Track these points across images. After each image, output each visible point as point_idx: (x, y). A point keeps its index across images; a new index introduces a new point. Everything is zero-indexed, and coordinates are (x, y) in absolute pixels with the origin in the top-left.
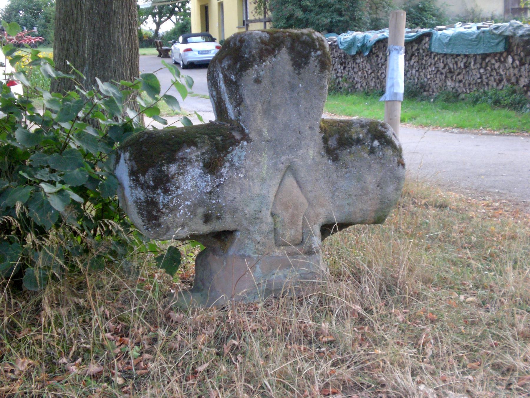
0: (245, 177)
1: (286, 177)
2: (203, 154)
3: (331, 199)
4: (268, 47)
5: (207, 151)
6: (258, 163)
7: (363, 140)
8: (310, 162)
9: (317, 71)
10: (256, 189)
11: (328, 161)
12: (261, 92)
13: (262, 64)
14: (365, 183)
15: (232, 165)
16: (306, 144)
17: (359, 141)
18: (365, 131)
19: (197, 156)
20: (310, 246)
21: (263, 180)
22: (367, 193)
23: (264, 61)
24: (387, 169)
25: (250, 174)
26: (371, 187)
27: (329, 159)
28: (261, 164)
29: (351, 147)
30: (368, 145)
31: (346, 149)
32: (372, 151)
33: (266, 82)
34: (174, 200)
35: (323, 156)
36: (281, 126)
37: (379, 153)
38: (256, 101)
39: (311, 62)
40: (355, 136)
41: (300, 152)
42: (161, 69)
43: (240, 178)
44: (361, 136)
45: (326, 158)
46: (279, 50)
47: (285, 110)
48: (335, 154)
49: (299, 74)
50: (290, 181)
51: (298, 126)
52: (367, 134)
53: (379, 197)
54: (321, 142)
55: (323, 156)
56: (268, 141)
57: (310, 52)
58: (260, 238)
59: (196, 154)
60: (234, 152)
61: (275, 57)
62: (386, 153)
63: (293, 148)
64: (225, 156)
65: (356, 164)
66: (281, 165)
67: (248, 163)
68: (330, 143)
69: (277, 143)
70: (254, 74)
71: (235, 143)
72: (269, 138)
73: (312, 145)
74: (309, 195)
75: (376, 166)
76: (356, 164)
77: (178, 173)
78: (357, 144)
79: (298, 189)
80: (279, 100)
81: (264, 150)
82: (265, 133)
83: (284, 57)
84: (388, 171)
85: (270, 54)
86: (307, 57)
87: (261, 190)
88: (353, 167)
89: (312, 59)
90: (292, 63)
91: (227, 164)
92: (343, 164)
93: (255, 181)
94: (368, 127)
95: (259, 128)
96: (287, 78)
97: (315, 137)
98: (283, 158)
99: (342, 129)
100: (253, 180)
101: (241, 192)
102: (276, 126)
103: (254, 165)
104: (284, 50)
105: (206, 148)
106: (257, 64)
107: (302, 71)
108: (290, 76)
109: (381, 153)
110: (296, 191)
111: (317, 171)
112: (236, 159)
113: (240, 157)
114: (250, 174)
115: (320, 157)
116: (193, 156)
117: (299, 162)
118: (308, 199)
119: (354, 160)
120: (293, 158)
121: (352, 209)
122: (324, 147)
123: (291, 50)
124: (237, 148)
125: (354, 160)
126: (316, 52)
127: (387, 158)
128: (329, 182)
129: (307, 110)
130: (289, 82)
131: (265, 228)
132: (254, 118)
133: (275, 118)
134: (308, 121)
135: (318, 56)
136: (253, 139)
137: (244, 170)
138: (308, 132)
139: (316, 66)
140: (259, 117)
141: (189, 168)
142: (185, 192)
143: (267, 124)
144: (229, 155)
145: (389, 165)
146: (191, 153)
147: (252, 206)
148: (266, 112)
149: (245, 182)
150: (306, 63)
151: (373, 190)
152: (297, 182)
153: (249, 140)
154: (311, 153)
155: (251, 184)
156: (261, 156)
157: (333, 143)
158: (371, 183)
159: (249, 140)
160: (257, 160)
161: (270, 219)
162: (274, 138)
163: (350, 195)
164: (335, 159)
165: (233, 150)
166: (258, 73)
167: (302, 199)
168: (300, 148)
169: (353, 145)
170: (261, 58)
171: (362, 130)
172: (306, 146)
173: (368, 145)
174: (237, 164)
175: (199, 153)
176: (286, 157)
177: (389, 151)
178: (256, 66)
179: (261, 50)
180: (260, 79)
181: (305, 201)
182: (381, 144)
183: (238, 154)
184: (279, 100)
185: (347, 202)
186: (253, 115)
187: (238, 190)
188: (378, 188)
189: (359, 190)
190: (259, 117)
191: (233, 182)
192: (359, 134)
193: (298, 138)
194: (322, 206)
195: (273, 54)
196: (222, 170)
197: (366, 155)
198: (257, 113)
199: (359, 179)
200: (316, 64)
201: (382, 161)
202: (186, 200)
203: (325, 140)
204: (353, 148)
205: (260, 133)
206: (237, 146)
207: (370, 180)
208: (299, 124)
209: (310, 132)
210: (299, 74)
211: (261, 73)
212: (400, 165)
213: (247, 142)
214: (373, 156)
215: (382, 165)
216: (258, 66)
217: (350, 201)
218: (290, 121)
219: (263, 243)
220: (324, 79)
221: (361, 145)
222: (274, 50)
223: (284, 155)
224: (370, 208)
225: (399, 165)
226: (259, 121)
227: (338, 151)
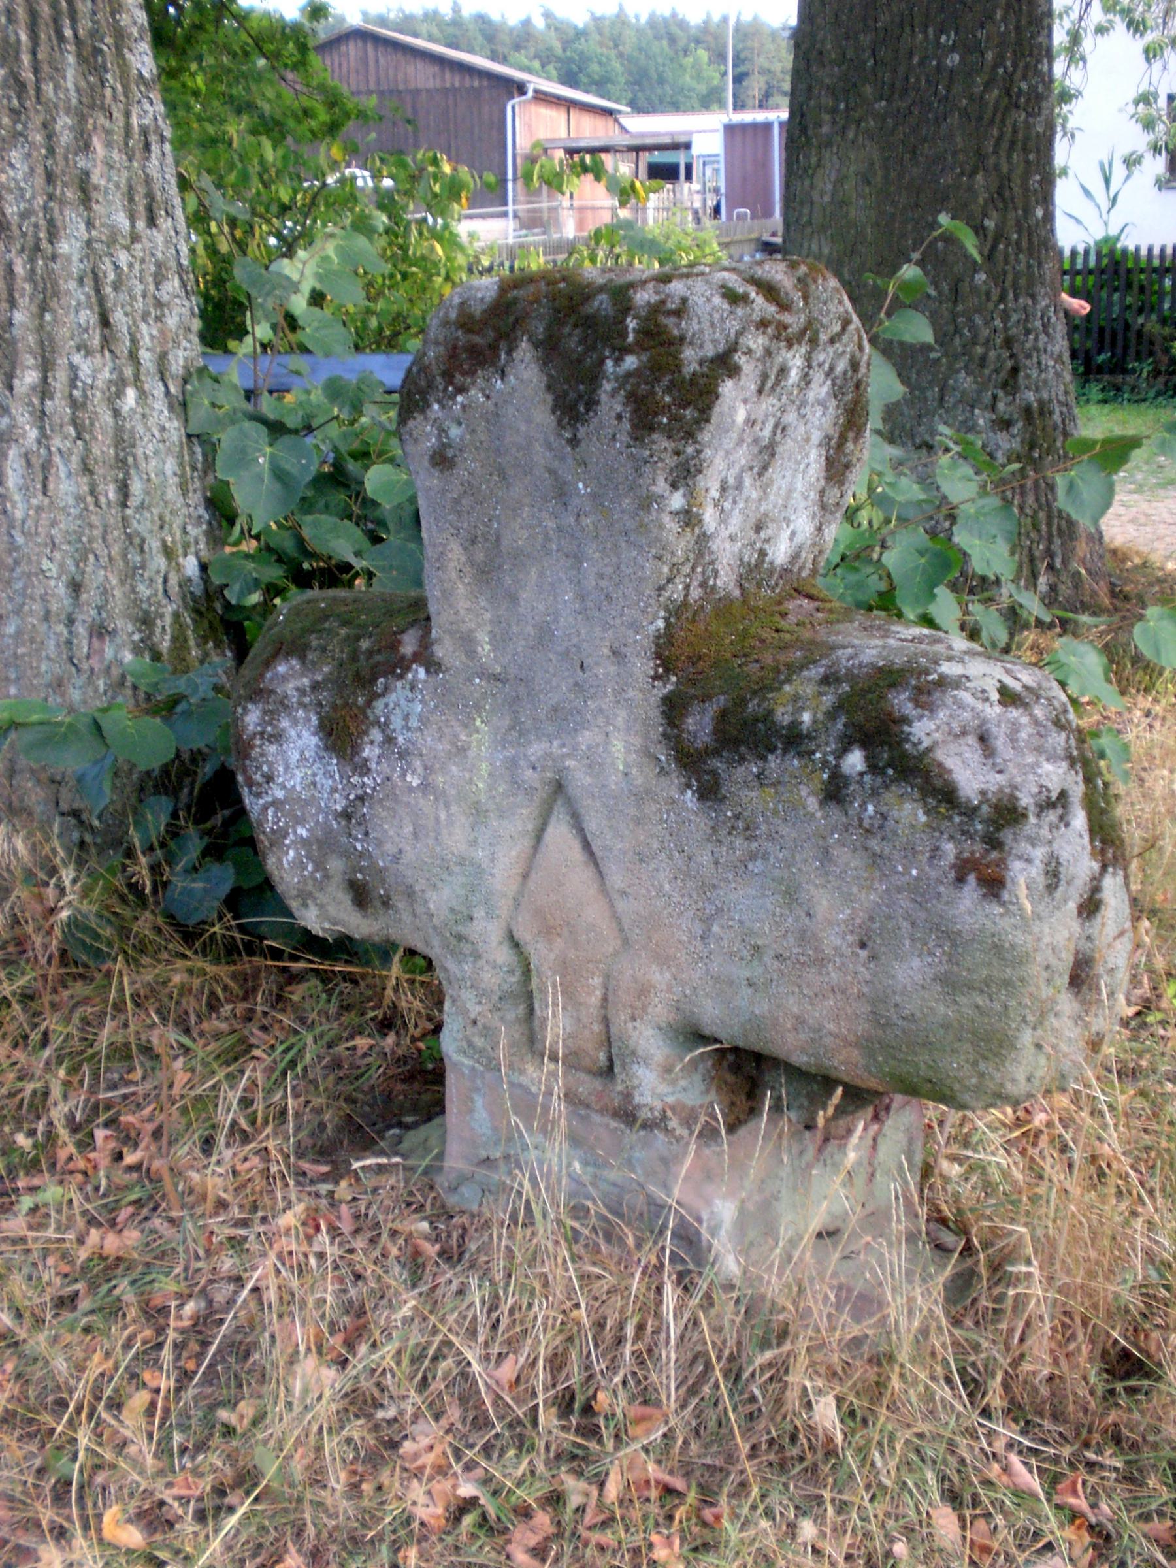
0: (425, 787)
1: (553, 820)
2: (315, 686)
3: (698, 943)
4: (477, 339)
5: (326, 680)
6: (462, 750)
7: (809, 737)
8: (614, 781)
9: (623, 438)
10: (456, 839)
11: (683, 793)
12: (457, 501)
13: (453, 398)
14: (809, 914)
15: (390, 740)
16: (601, 710)
17: (794, 740)
18: (828, 700)
19: (302, 692)
20: (628, 1096)
21: (478, 813)
22: (820, 962)
23: (461, 390)
24: (896, 880)
26: (833, 940)
27: (689, 786)
28: (471, 754)
29: (764, 758)
30: (825, 763)
31: (742, 759)
32: (835, 791)
33: (470, 465)
34: (270, 812)
35: (663, 772)
36: (530, 629)
37: (863, 806)
38: (441, 530)
39: (604, 398)
40: (783, 716)
41: (586, 738)
42: (1078, 221)
43: (411, 789)
44: (806, 717)
45: (676, 779)
46: (509, 352)
47: (541, 574)
48: (709, 772)
49: (574, 442)
51: (575, 640)
52: (832, 715)
53: (865, 990)
54: (655, 714)
55: (663, 772)
56: (496, 678)
57: (602, 362)
58: (478, 1008)
59: (298, 683)
60: (392, 698)
61: (503, 375)
62: (895, 813)
63: (564, 719)
64: (369, 704)
65: (785, 830)
66: (529, 772)
67: (428, 741)
68: (691, 723)
69: (522, 691)
70: (428, 436)
71: (397, 666)
72: (499, 669)
74: (621, 905)
75: (848, 859)
76: (785, 830)
77: (262, 733)
78: (785, 751)
79: (588, 873)
80: (525, 534)
81: (478, 707)
82: (485, 648)
83: (524, 375)
84: (899, 890)
85: (482, 364)
86: (594, 377)
87: (474, 843)
88: (770, 838)
89: (607, 386)
90: (550, 398)
91: (376, 734)
92: (737, 817)
93: (454, 809)
94: (846, 687)
95: (463, 628)
96: (541, 456)
97: (631, 693)
98: (536, 749)
100: (447, 806)
101: (415, 835)
102: (515, 629)
103: (449, 755)
104: (525, 350)
105: (326, 669)
106: (439, 402)
107: (582, 431)
108: (549, 446)
109: (870, 808)
110: (580, 878)
111: (638, 822)
112: (397, 722)
113: (406, 717)
115: (652, 771)
116: (290, 688)
118: (616, 917)
119: (775, 812)
120: (564, 756)
121: (762, 1008)
122: (664, 735)
123: (549, 348)
124: (399, 684)
125: (775, 812)
126: (618, 361)
127: (895, 833)
128: (687, 875)
129: (604, 583)
130: (552, 472)
131: (490, 979)
132: (443, 592)
133: (513, 599)
134: (606, 627)
135: (629, 374)
136: (447, 663)
137: (417, 764)
138: (605, 669)
139: (619, 417)
140: (461, 590)
141: (285, 723)
142: (292, 797)
143: (488, 616)
144: (379, 704)
145: (907, 870)
146: (284, 678)
147: (446, 892)
148: (486, 574)
149: (425, 804)
150: (592, 404)
151: (842, 956)
152: (586, 846)
153: (433, 666)
154: (618, 746)
155: (443, 816)
156: (466, 726)
157: (699, 725)
158: (830, 923)
159: (433, 666)
160: (456, 736)
161: (503, 955)
162: (513, 671)
163: (757, 948)
164: (709, 792)
165: (387, 689)
166: (442, 431)
167: (595, 913)
168: (584, 725)
169: (772, 750)
170: (448, 376)
171: (820, 694)
172: (601, 720)
173: (825, 763)
174: (400, 739)
175: (306, 681)
176: (545, 745)
177: (908, 806)
178: (436, 407)
179: (453, 353)
180: (450, 453)
181: (605, 925)
182: (873, 767)
183: (403, 703)
184: (525, 534)
185: (747, 974)
186: (441, 581)
187: (408, 829)
188: (864, 954)
189: (791, 940)
190: (461, 590)
191: (396, 800)
192: (803, 709)
193: (576, 684)
194: (663, 960)
195: (493, 364)
196: (366, 753)
197: (812, 803)
198: (454, 575)
199: (791, 895)
200: (619, 408)
201: (874, 844)
202: (300, 821)
204: (773, 762)
205: (467, 642)
206: (401, 677)
207: (833, 910)
208: (579, 634)
209: (613, 669)
210: (574, 442)
211: (455, 432)
212: (972, 879)
213: (427, 672)
214: (835, 812)
215: (876, 859)
216: (443, 407)
218: (556, 615)
219: (485, 1027)
220: (647, 469)
221: (800, 755)
222: (494, 348)
223: (538, 738)
224: (831, 1027)
225: (960, 880)
226: (463, 605)
227: (716, 763)
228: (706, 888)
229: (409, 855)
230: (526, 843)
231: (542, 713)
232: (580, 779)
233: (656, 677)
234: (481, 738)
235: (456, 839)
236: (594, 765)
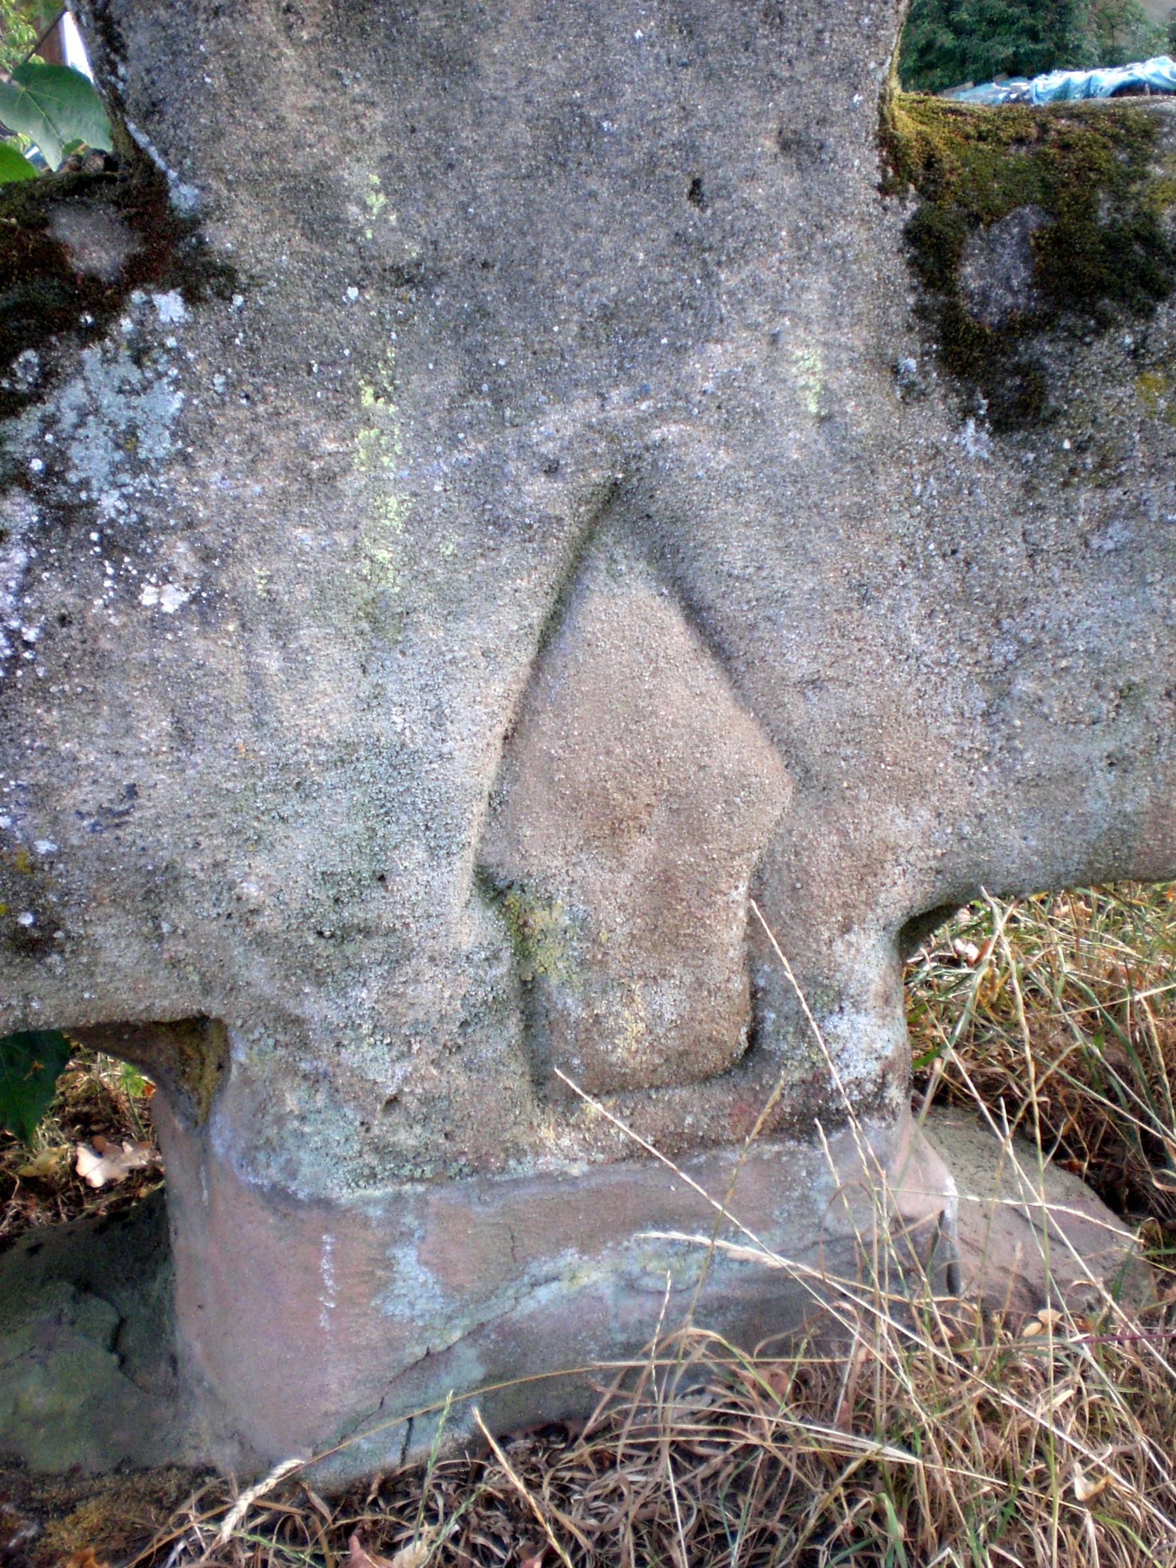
0: (204, 606)
1: (597, 581)
3: (979, 730)
8: (797, 442)
10: (324, 701)
16: (757, 287)
20: (817, 1081)
21: (383, 623)
25: (255, 576)
27: (968, 412)
28: (349, 484)
29: (1147, 313)
31: (1104, 323)
36: (518, 129)
43: (158, 622)
45: (940, 404)
48: (1017, 370)
50: (628, 609)
51: (675, 132)
54: (896, 266)
55: (912, 393)
56: (403, 276)
58: (405, 1067)
63: (634, 333)
66: (538, 486)
68: (970, 274)
69: (491, 289)
72: (414, 250)
73: (813, 301)
74: (800, 710)
79: (707, 673)
81: (365, 360)
92: (1080, 448)
93: (307, 634)
95: (298, 163)
97: (842, 231)
98: (556, 425)
99: (1072, 159)
100: (282, 632)
101: (182, 736)
102: (467, 137)
103: (282, 503)
110: (690, 690)
111: (857, 517)
112: (92, 458)
113: (127, 438)
114: (255, 576)
115: (887, 397)
117: (697, 451)
118: (789, 748)
122: (921, 311)
124: (91, 355)
128: (966, 598)
131: (435, 993)
134: (769, 84)
136: (246, 264)
137: (181, 554)
138: (771, 185)
143: (377, 117)
147: (301, 843)
149: (215, 650)
152: (695, 613)
154: (806, 363)
155: (272, 662)
156: (337, 415)
157: (993, 275)
160: (306, 449)
161: (472, 928)
162: (461, 244)
163: (1128, 694)
165: (49, 377)
167: (739, 746)
168: (707, 330)
172: (756, 311)
174: (110, 503)
176: (584, 409)
181: (767, 767)
185: (1109, 745)
186: (225, 42)
187: (154, 728)
191: (100, 663)
193: (679, 238)
194: (910, 789)
203: (931, 252)
205: (312, 203)
206: (96, 333)
208: (687, 113)
209: (789, 183)
213: (191, 298)
217: (1131, 733)
218: (605, 85)
223: (562, 397)
226: (294, 101)
227: (1044, 347)
228: (999, 610)
229: (162, 786)
230: (526, 654)
231: (566, 334)
233: (883, 189)
235: (324, 701)
236: (740, 415)
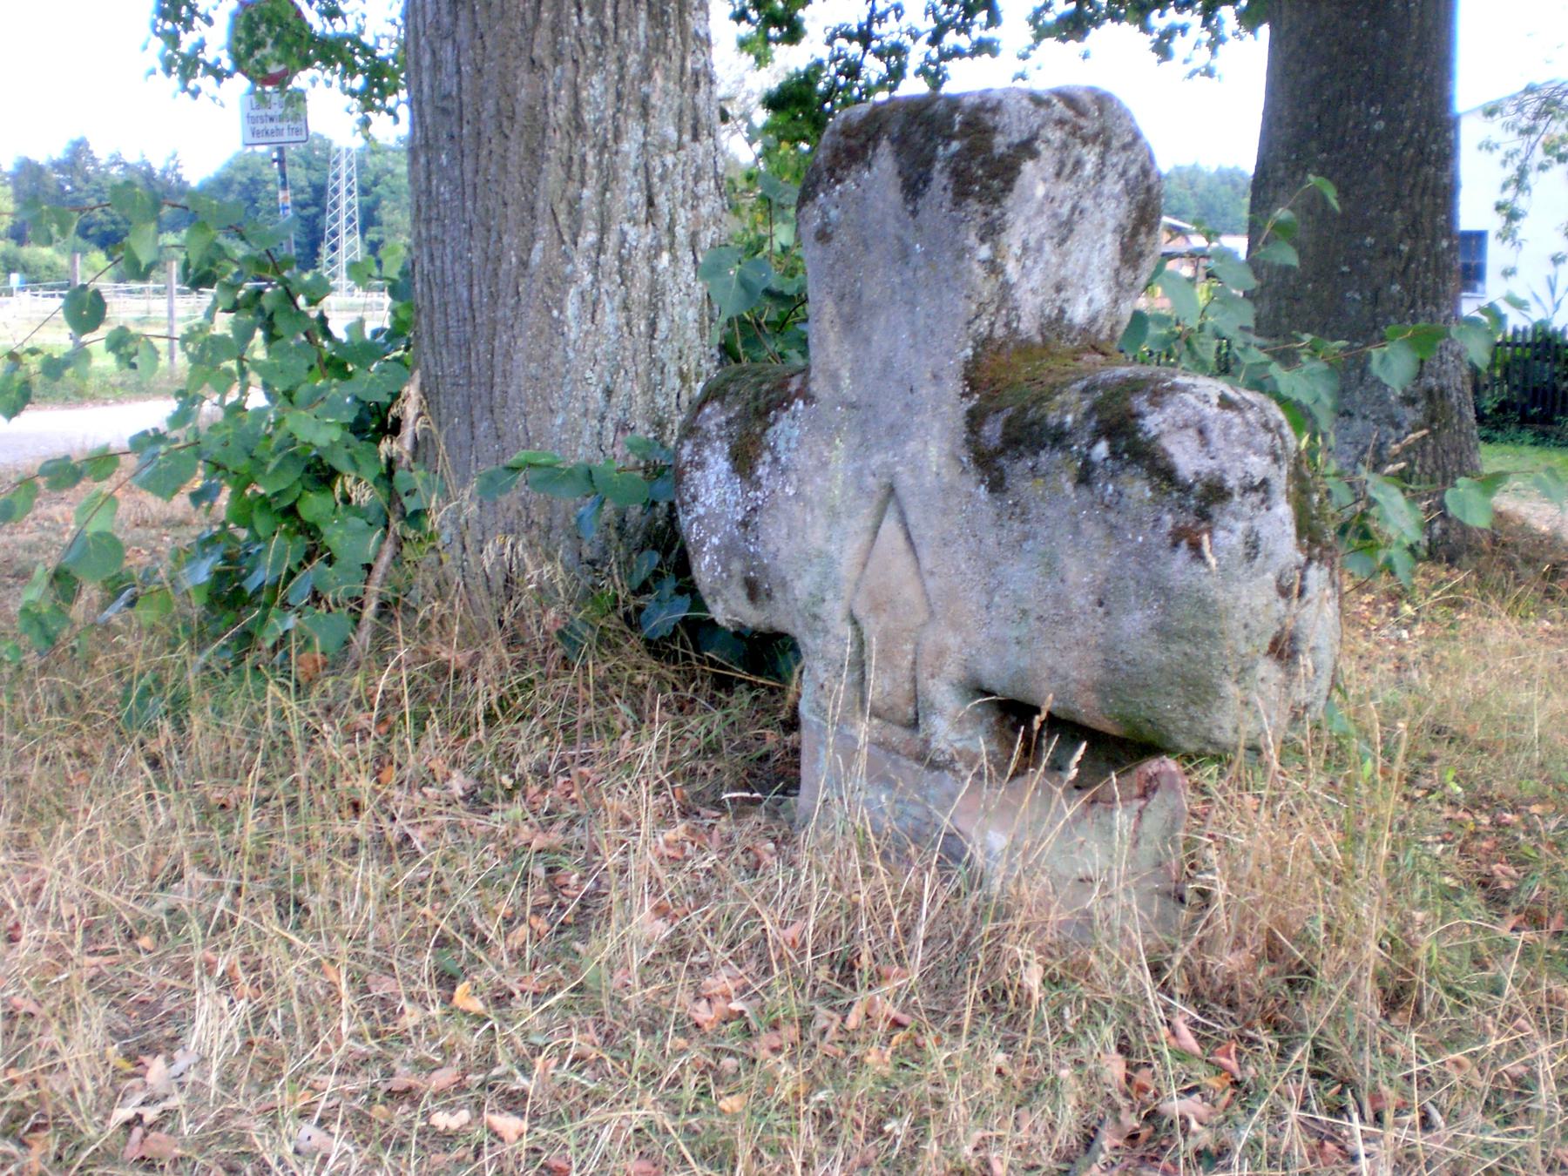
2: (729, 422)
4: (853, 142)
6: (825, 465)
7: (1070, 434)
8: (929, 480)
9: (947, 204)
10: (816, 537)
12: (832, 267)
15: (776, 460)
17: (1059, 437)
18: (1086, 404)
20: (926, 742)
21: (834, 514)
22: (1069, 620)
23: (839, 181)
24: (1128, 547)
25: (808, 489)
29: (1036, 454)
30: (1080, 453)
31: (1021, 455)
32: (1085, 477)
33: (842, 238)
39: (935, 174)
40: (1052, 419)
41: (912, 447)
43: (788, 498)
44: (1069, 418)
45: (974, 476)
49: (914, 213)
50: (890, 526)
52: (1088, 415)
54: (960, 424)
55: (964, 471)
56: (853, 406)
60: (779, 426)
63: (897, 433)
67: (802, 460)
68: (987, 430)
71: (782, 401)
73: (935, 431)
74: (931, 583)
81: (838, 429)
82: (846, 383)
84: (1129, 554)
86: (929, 162)
87: (828, 539)
88: (1039, 520)
89: (938, 166)
91: (767, 457)
94: (1100, 393)
96: (892, 227)
98: (876, 460)
103: (816, 469)
104: (885, 147)
107: (920, 202)
108: (897, 218)
110: (901, 564)
112: (781, 445)
114: (808, 489)
116: (711, 425)
118: (925, 594)
121: (1025, 662)
122: (967, 441)
123: (901, 143)
125: (1043, 498)
130: (900, 239)
137: (794, 477)
138: (926, 391)
140: (832, 336)
141: (707, 453)
144: (770, 431)
146: (709, 418)
147: (807, 580)
148: (849, 323)
149: (796, 509)
150: (927, 181)
152: (908, 537)
153: (809, 399)
154: (933, 451)
157: (992, 431)
159: (809, 399)
161: (847, 631)
163: (1024, 612)
164: (997, 486)
165: (776, 419)
166: (825, 213)
167: (910, 592)
170: (831, 171)
177: (1138, 484)
182: (1114, 454)
183: (787, 430)
185: (1015, 634)
187: (784, 531)
188: (1101, 610)
190: (832, 336)
194: (956, 626)
197: (1069, 487)
202: (714, 532)
203: (974, 419)
204: (1044, 456)
205: (834, 378)
207: (1079, 576)
209: (933, 389)
211: (833, 213)
212: (1184, 544)
214: (1084, 492)
215: (1113, 529)
217: (1023, 631)
222: (864, 147)
224: (1074, 674)
225: (1175, 545)
226: (832, 349)
227: (1003, 461)
228: (992, 565)
229: (784, 553)
230: (866, 537)
231: (882, 430)
232: (906, 481)
233: (963, 395)
234: (839, 455)
235: (816, 537)
236: (917, 469)
